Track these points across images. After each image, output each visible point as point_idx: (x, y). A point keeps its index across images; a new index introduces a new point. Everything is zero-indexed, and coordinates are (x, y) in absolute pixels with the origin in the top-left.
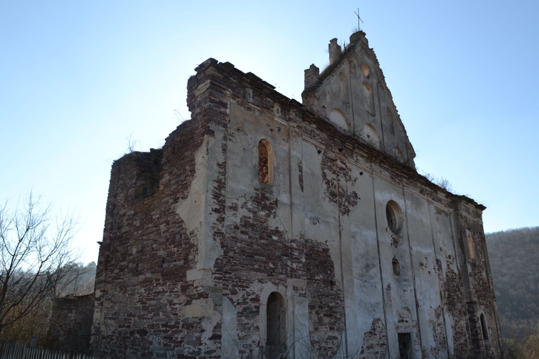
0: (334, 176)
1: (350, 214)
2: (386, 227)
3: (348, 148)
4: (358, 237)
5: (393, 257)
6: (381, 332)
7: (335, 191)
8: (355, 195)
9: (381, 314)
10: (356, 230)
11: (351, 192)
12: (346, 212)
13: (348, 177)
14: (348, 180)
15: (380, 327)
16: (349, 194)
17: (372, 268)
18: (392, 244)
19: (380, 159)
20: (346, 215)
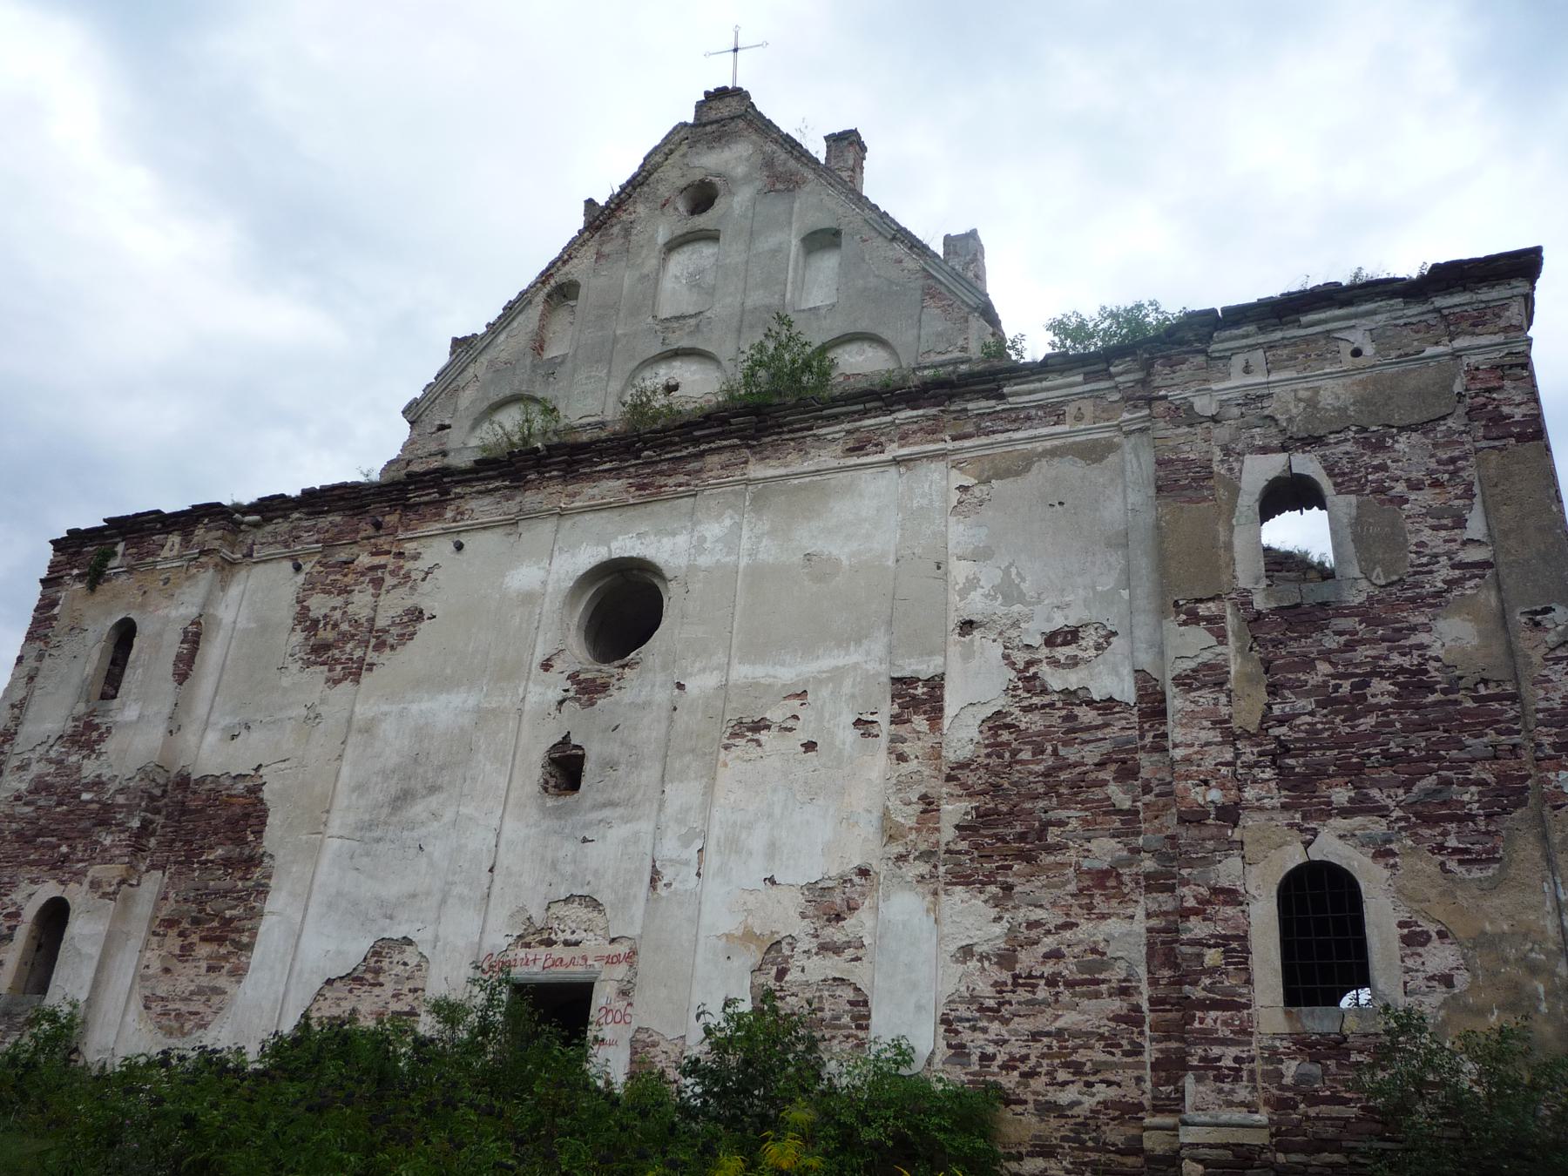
0: (338, 601)
1: (366, 678)
2: (539, 657)
3: (426, 504)
4: (387, 728)
5: (559, 739)
6: (408, 978)
7: (328, 635)
8: (417, 615)
9: (419, 925)
10: (385, 708)
11: (400, 612)
12: (355, 671)
13: (390, 581)
14: (394, 587)
15: (405, 964)
16: (381, 623)
17: (424, 797)
18: (561, 703)
19: (555, 463)
20: (347, 685)
